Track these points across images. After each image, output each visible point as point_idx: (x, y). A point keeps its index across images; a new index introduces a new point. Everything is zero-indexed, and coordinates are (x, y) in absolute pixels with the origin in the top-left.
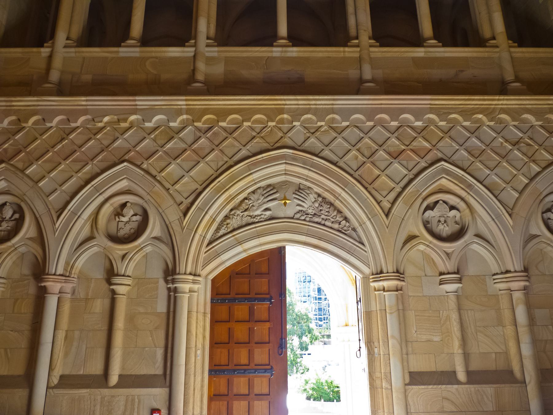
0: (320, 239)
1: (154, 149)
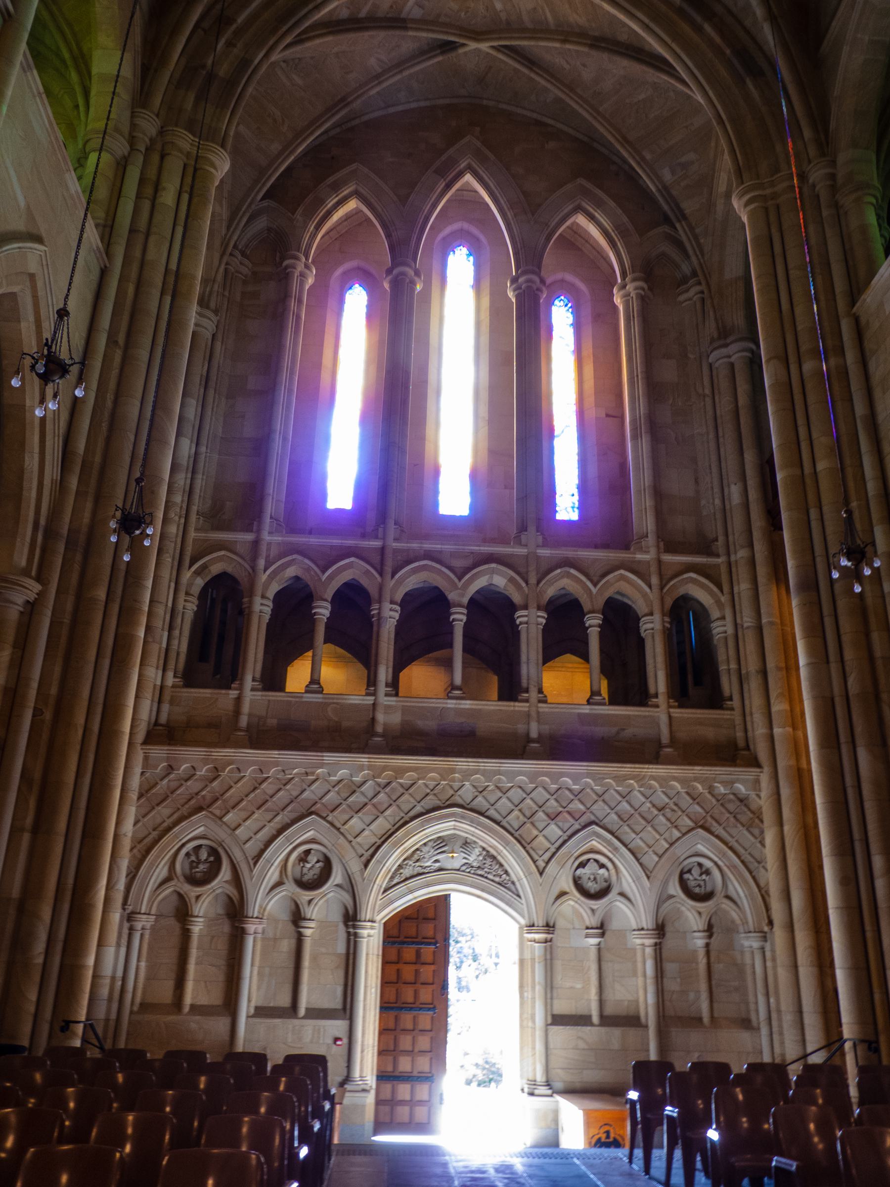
0: (483, 890)
1: (338, 802)
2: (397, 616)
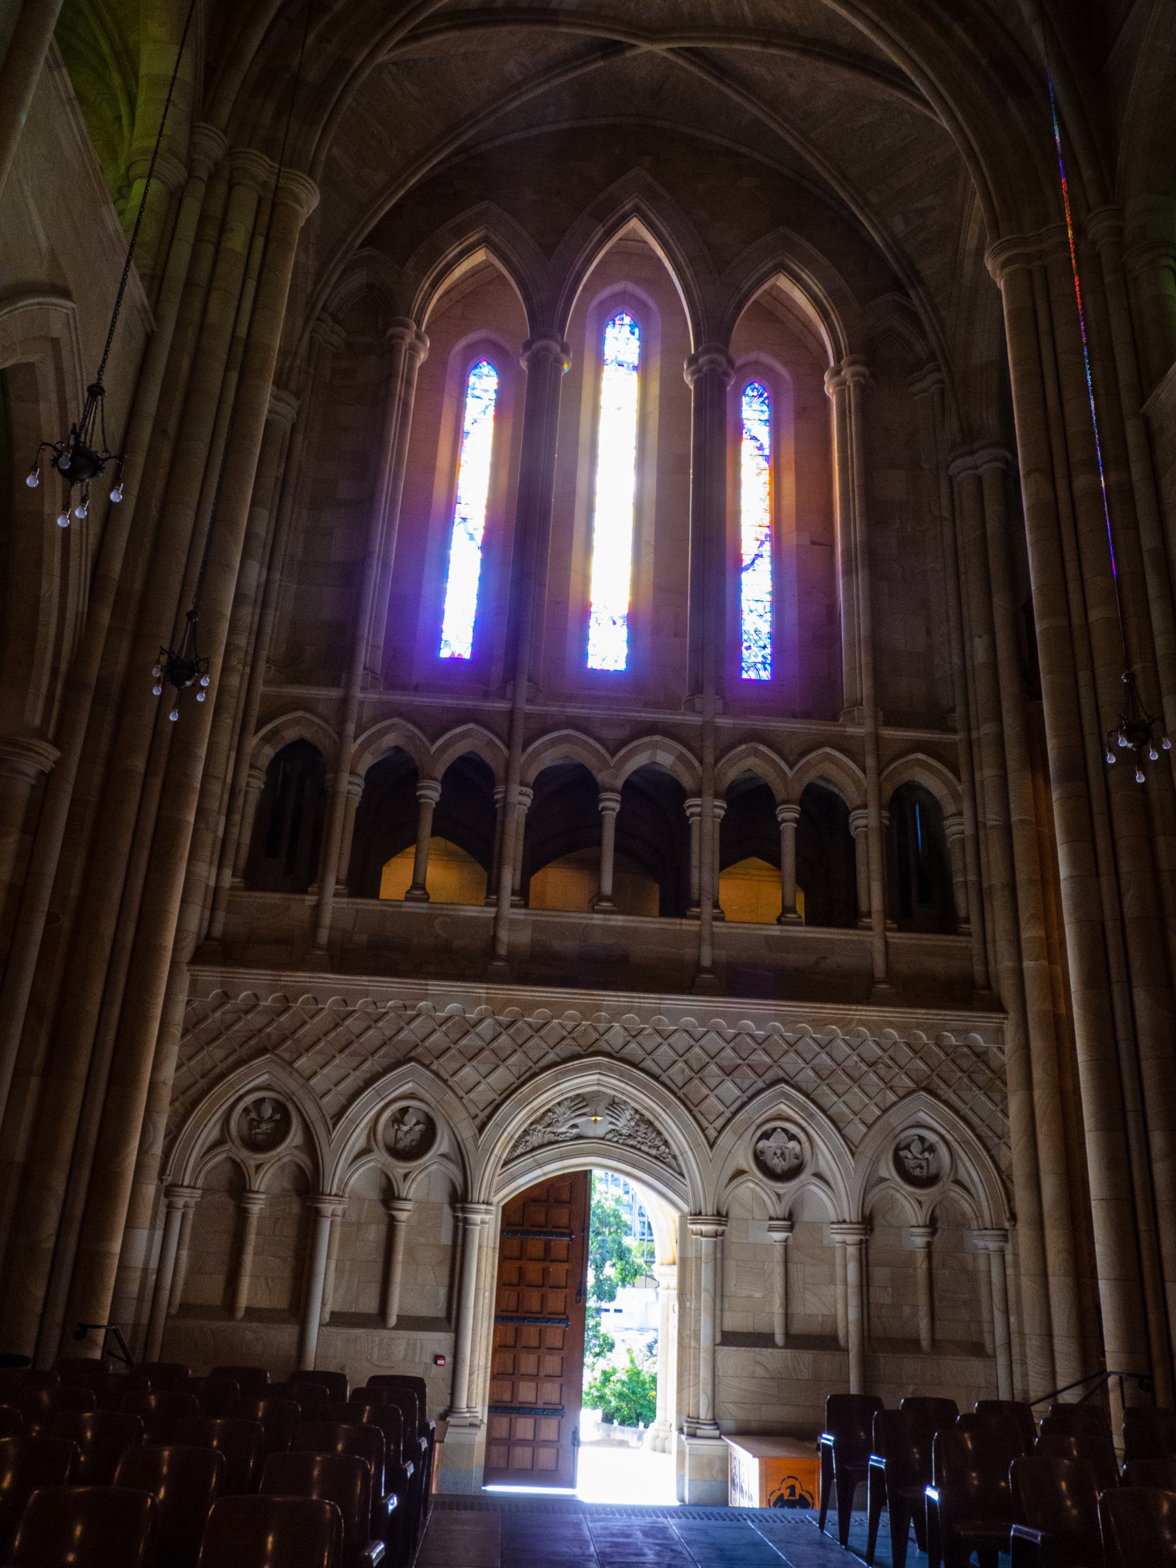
0: (634, 1166)
2: (528, 801)
